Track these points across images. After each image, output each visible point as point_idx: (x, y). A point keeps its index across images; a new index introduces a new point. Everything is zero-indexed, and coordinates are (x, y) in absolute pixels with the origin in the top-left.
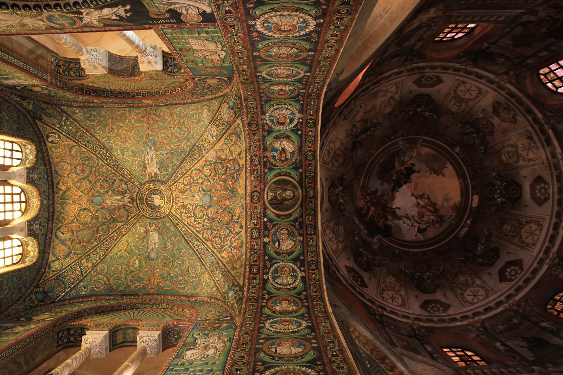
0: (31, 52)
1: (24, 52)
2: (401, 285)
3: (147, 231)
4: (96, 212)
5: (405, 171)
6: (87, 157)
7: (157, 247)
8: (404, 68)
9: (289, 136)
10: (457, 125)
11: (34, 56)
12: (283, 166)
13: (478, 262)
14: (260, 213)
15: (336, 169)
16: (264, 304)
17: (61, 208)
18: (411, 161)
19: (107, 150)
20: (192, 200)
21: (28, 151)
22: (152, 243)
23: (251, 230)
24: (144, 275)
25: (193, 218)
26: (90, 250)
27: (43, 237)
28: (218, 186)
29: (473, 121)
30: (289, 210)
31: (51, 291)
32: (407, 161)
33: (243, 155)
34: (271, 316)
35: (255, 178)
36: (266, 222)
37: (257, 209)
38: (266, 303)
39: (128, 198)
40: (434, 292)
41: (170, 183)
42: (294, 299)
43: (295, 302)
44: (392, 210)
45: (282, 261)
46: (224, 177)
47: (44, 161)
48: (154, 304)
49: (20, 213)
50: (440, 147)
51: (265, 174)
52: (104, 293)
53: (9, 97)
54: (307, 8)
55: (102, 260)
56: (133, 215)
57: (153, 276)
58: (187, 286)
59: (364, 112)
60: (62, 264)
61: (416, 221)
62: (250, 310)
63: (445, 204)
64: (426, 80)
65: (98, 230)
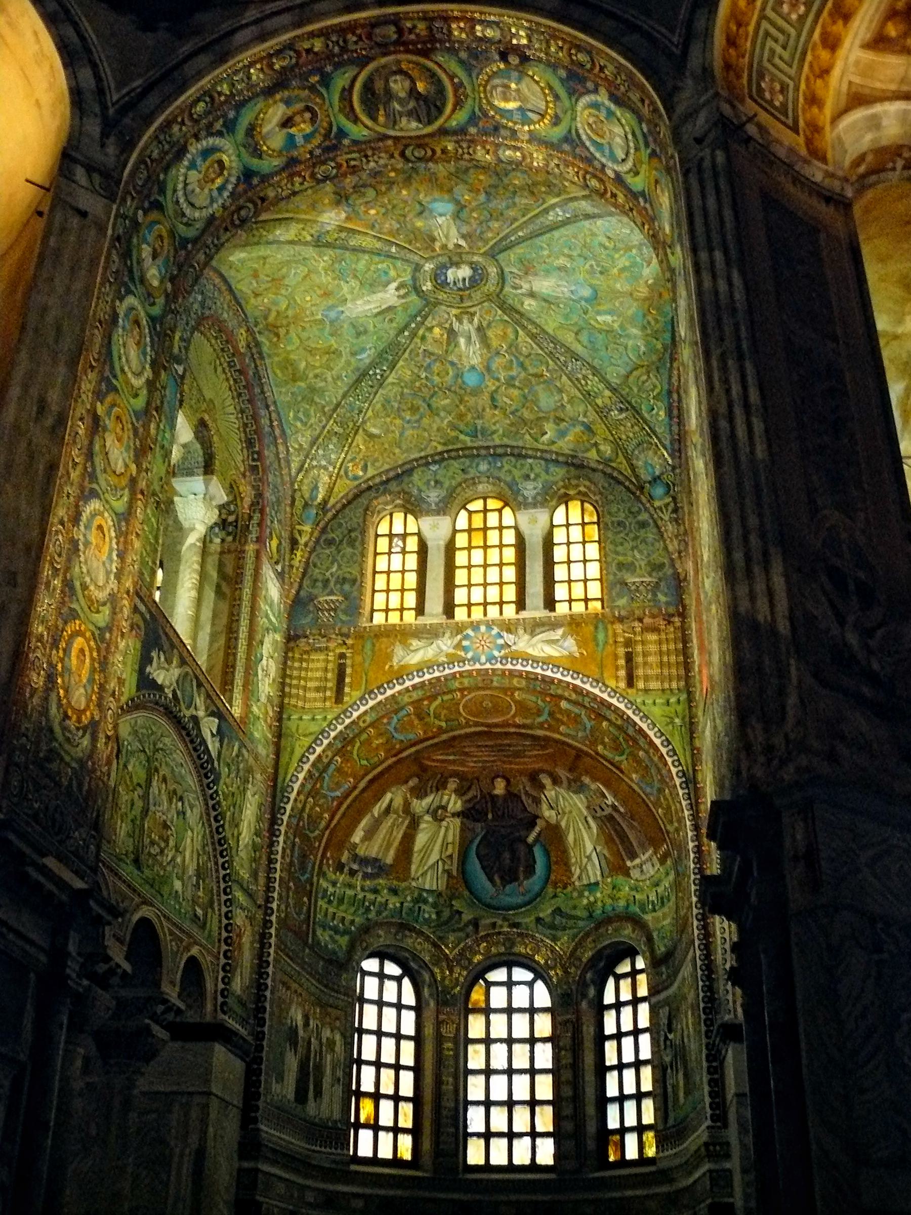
0: (219, 592)
1: (224, 607)
3: (532, 295)
6: (383, 406)
9: (247, 129)
11: (224, 585)
14: (457, 142)
17: (495, 436)
19: (363, 375)
20: (448, 228)
21: (388, 507)
24: (629, 308)
27: (553, 468)
31: (653, 468)
35: (368, 161)
39: (461, 322)
41: (416, 258)
47: (403, 473)
49: (507, 512)
51: (355, 142)
52: (665, 377)
53: (297, 569)
54: (77, 584)
55: (595, 371)
56: (500, 312)
57: (631, 295)
60: (605, 439)
65: (535, 375)
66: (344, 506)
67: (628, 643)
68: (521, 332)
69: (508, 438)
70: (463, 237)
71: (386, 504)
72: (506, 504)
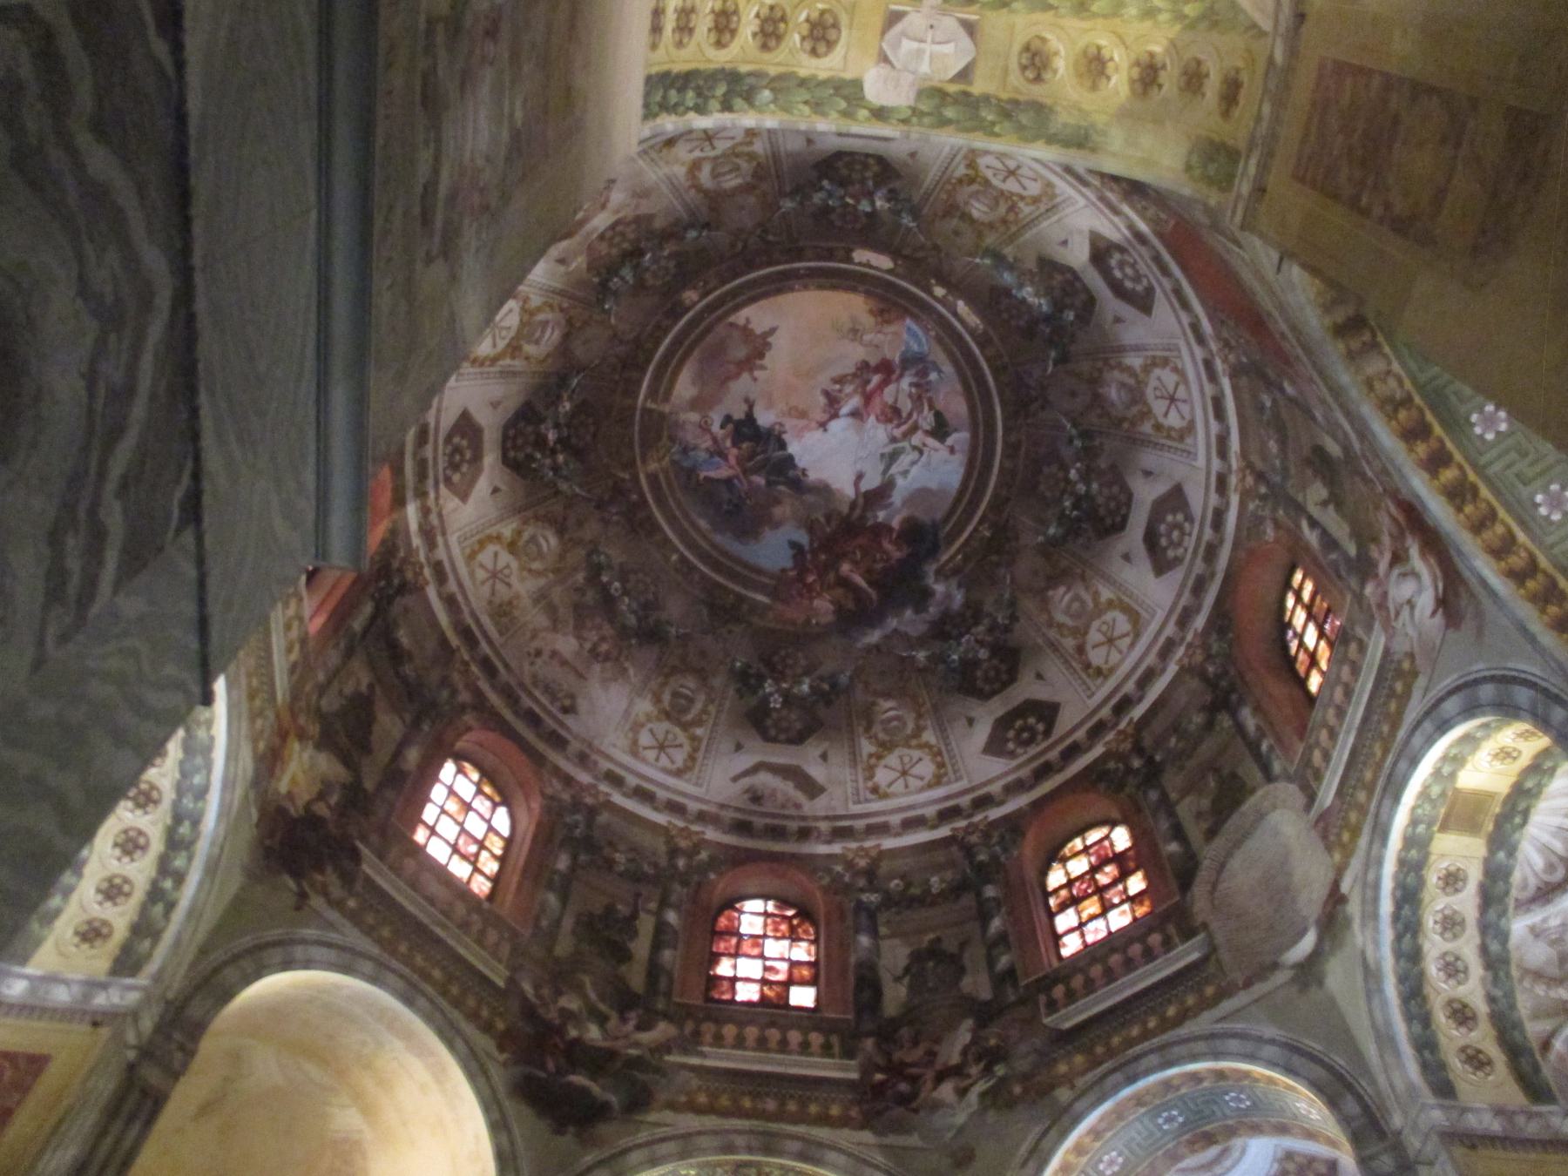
2: (1083, 578)
5: (745, 446)
8: (427, 572)
10: (604, 311)
13: (1072, 323)
15: (712, 701)
18: (716, 428)
29: (599, 274)
32: (715, 440)
40: (1130, 496)
44: (861, 501)
50: (677, 342)
59: (555, 629)
61: (907, 435)
63: (867, 337)
64: (455, 467)
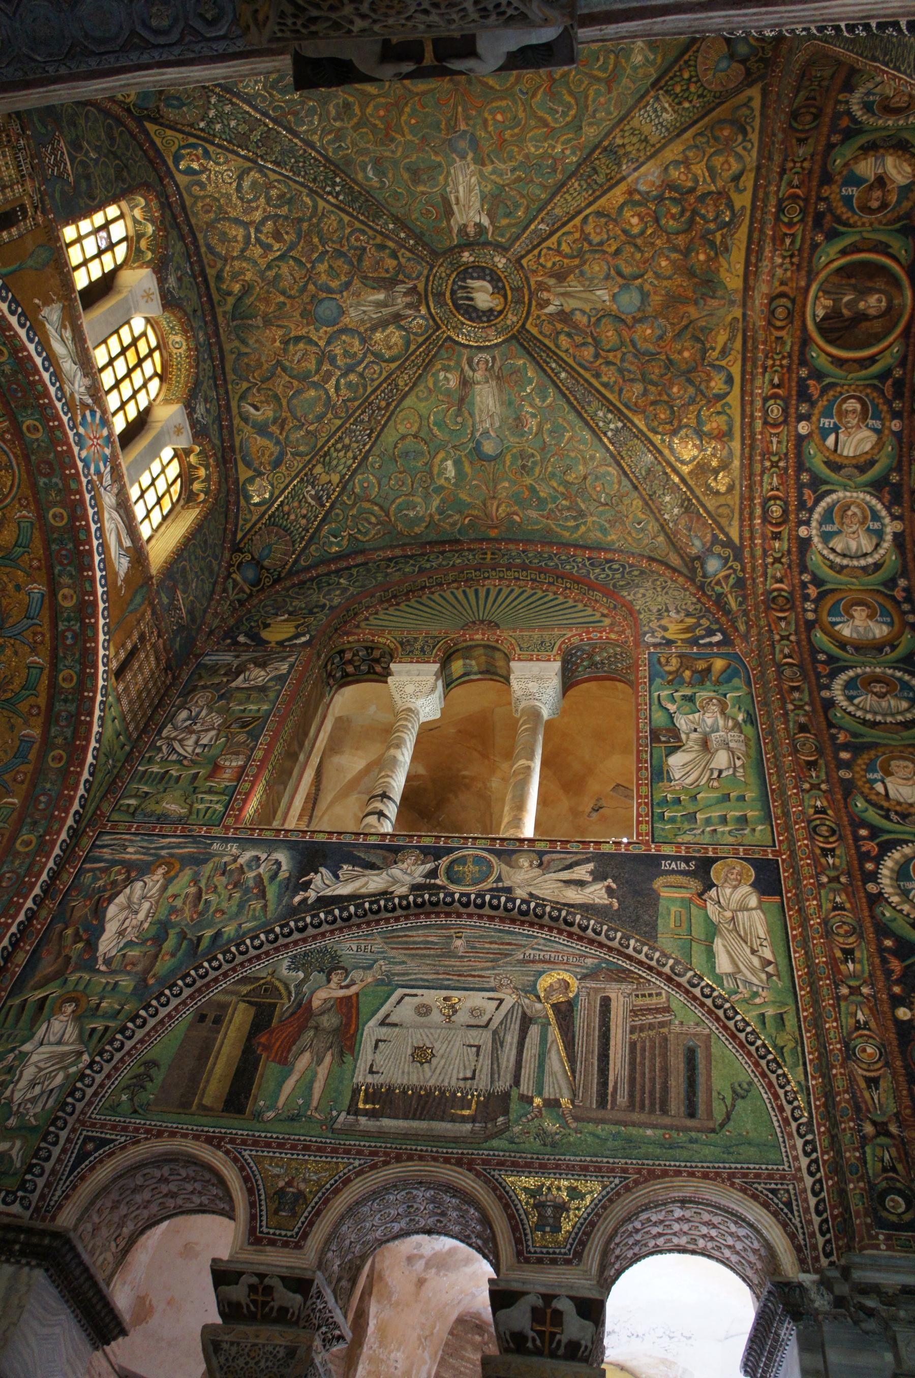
3: (465, 383)
4: (328, 343)
7: (497, 425)
12: (871, 224)
14: (790, 356)
16: (810, 616)
17: (237, 343)
20: (586, 300)
21: (137, 213)
22: (484, 417)
23: (765, 400)
24: (470, 495)
25: (592, 350)
26: (328, 441)
28: (664, 264)
30: (869, 345)
31: (268, 556)
33: (748, 181)
34: (838, 659)
35: (784, 258)
36: (805, 379)
37: (784, 343)
38: (815, 611)
39: (405, 294)
42: (881, 600)
43: (885, 612)
45: (845, 487)
46: (681, 241)
47: (178, 226)
48: (509, 569)
49: (156, 382)
51: (815, 246)
56: (421, 340)
58: (585, 523)
62: (783, 638)
66: (141, 146)
67: (142, 637)
68: (393, 366)
69: (237, 359)
70: (562, 312)
71: (147, 209)
72: (162, 378)
